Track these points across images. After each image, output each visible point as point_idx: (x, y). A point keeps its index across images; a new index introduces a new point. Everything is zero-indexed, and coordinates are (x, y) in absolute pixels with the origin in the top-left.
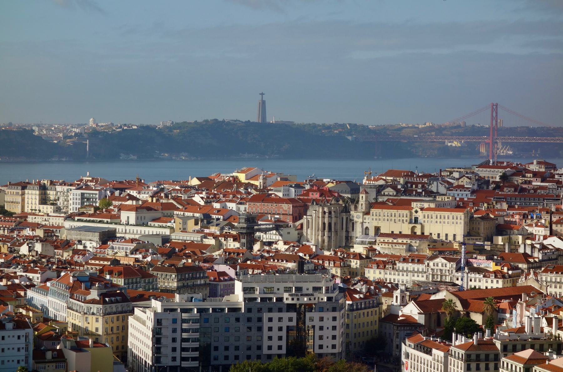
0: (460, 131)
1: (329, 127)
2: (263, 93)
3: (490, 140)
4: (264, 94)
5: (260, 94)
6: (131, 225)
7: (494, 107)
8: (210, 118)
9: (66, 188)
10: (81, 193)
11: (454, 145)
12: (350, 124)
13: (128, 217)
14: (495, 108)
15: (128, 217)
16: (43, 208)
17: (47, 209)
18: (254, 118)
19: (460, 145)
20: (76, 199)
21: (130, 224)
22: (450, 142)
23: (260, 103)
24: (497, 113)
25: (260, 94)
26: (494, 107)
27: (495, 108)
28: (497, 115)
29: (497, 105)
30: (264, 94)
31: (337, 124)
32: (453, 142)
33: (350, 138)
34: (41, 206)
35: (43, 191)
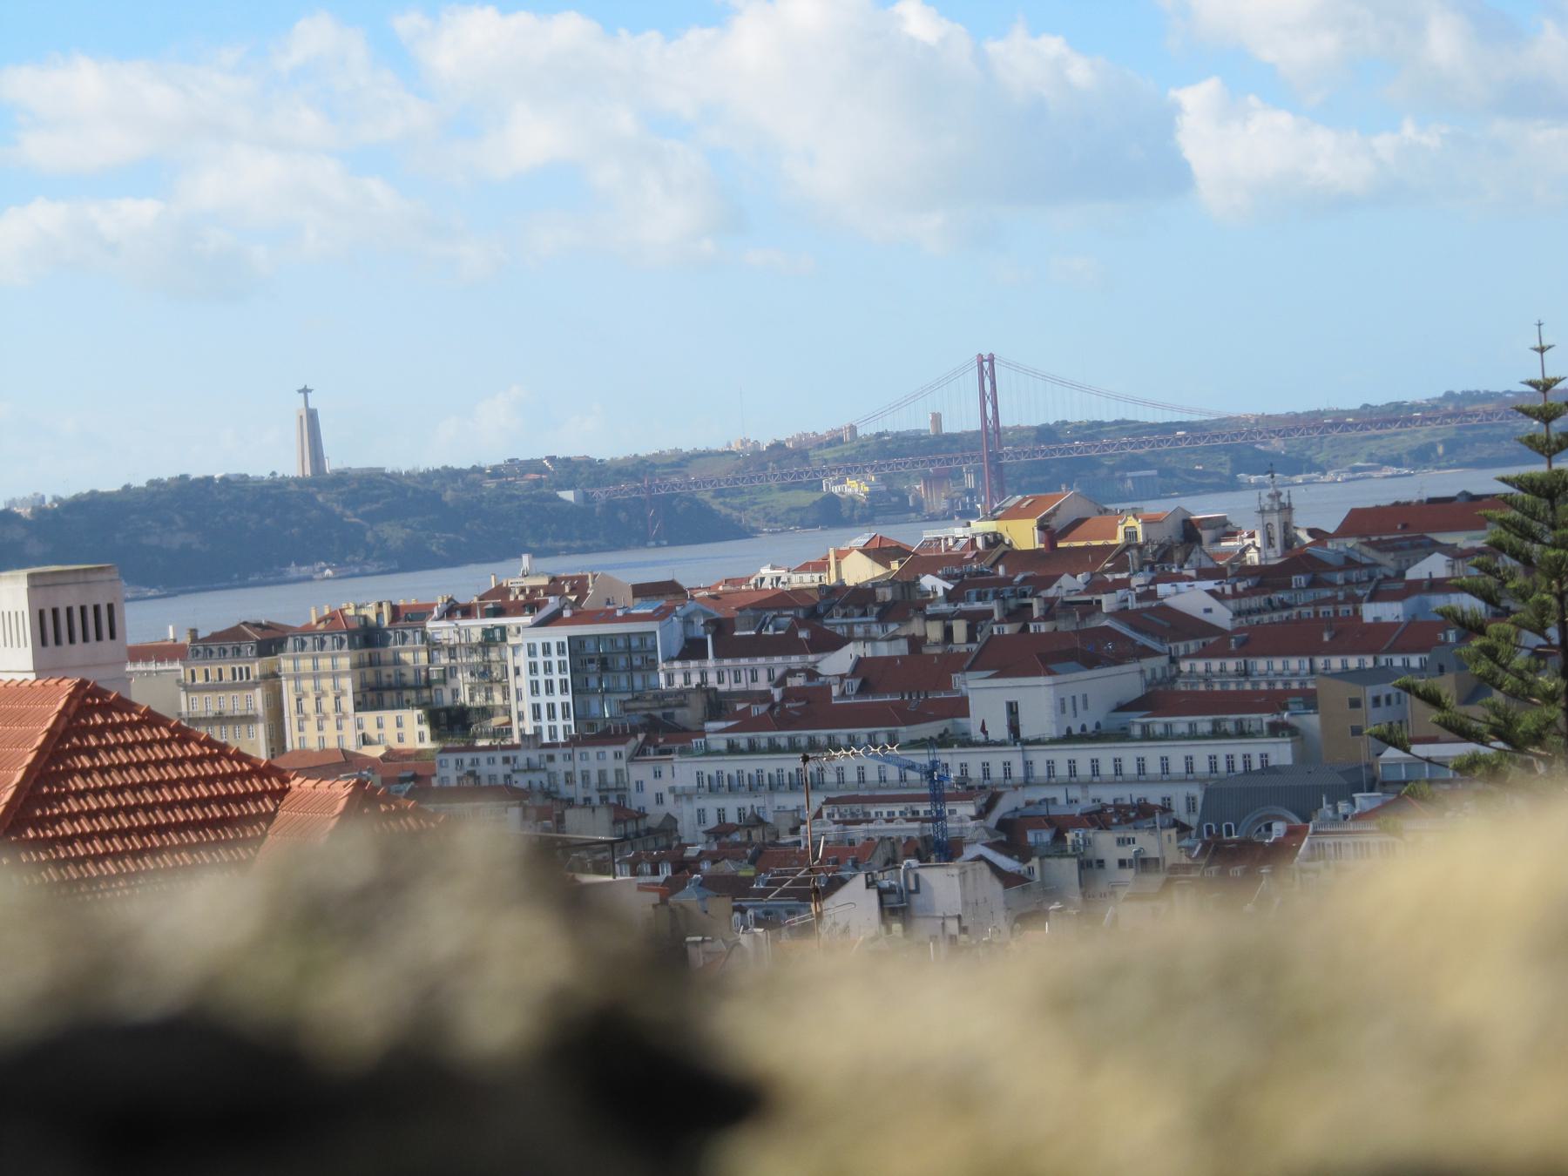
0: (846, 454)
1: (496, 472)
2: (308, 387)
3: (983, 461)
4: (310, 391)
5: (300, 391)
6: (996, 744)
7: (986, 365)
8: (167, 471)
9: (475, 627)
10: (569, 638)
12: (552, 459)
13: (1012, 709)
14: (986, 366)
15: (1012, 709)
16: (380, 726)
17: (399, 725)
18: (288, 463)
19: (867, 489)
20: (548, 668)
21: (1025, 733)
22: (836, 483)
23: (301, 417)
24: (993, 383)
25: (300, 391)
26: (986, 365)
27: (986, 366)
29: (991, 359)
30: (310, 391)
31: (517, 462)
33: (568, 495)
34: (369, 718)
35: (366, 652)
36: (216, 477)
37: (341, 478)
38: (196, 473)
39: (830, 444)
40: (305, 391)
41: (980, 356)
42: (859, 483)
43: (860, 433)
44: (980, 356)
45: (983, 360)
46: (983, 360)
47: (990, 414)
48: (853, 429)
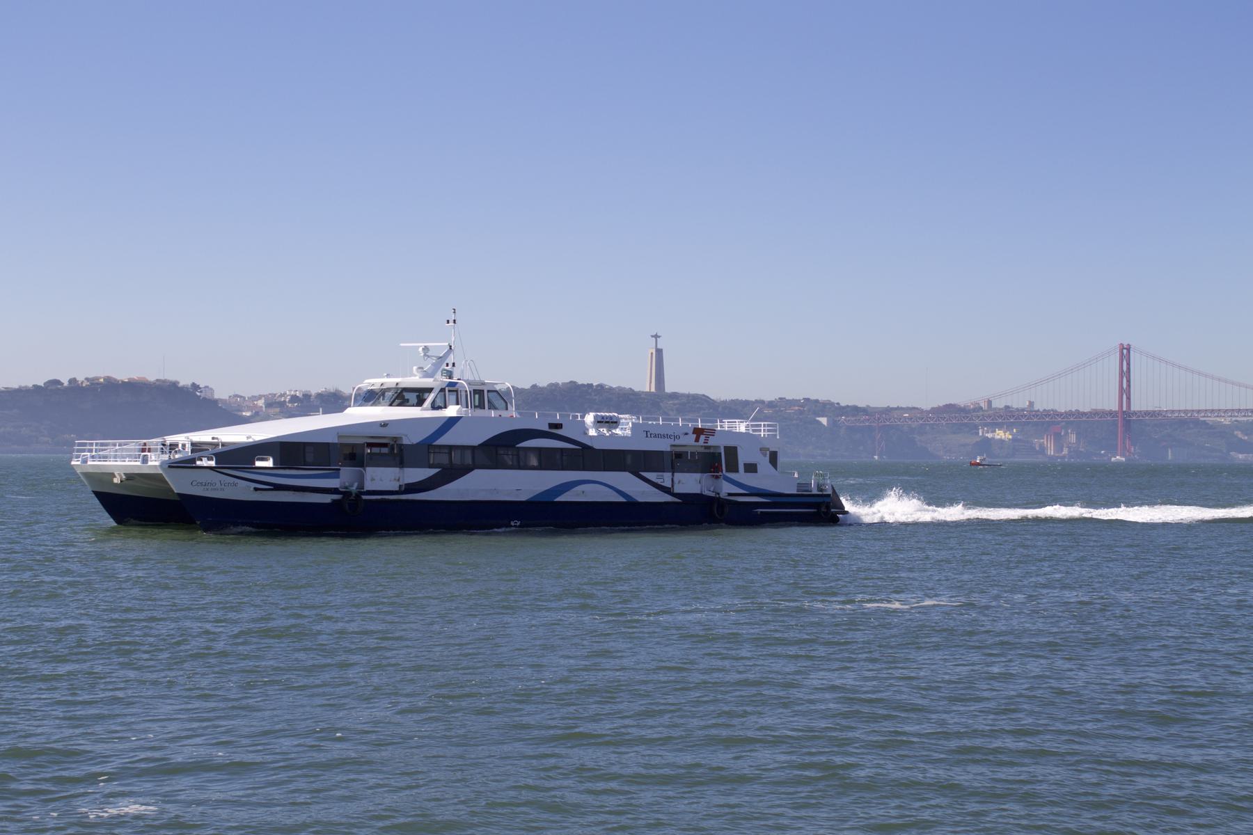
3: (1117, 417)
4: (659, 337)
5: (652, 336)
7: (1125, 351)
11: (999, 437)
14: (1125, 352)
19: (1010, 437)
23: (652, 353)
24: (1128, 364)
25: (652, 336)
26: (1125, 351)
27: (1125, 352)
28: (1129, 368)
30: (659, 337)
32: (995, 431)
33: (824, 420)
36: (594, 384)
37: (674, 396)
38: (581, 380)
39: (974, 410)
40: (656, 337)
41: (1122, 345)
42: (1005, 432)
43: (994, 406)
44: (1122, 347)
45: (1123, 348)
46: (1123, 348)
47: (1125, 386)
48: (990, 402)
